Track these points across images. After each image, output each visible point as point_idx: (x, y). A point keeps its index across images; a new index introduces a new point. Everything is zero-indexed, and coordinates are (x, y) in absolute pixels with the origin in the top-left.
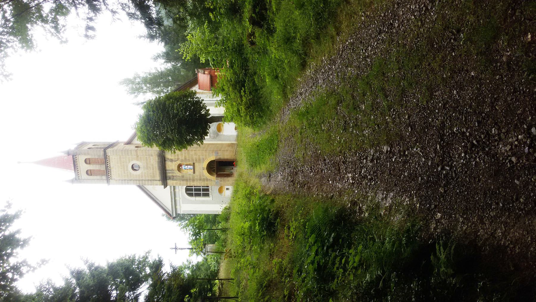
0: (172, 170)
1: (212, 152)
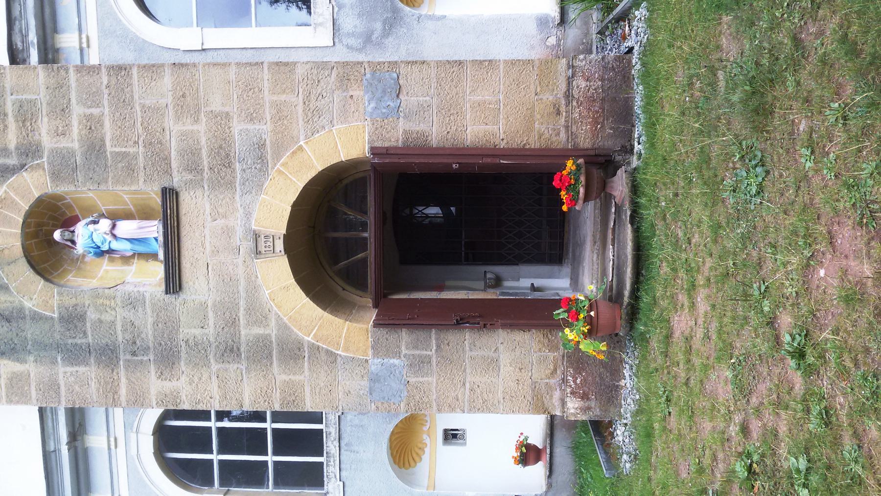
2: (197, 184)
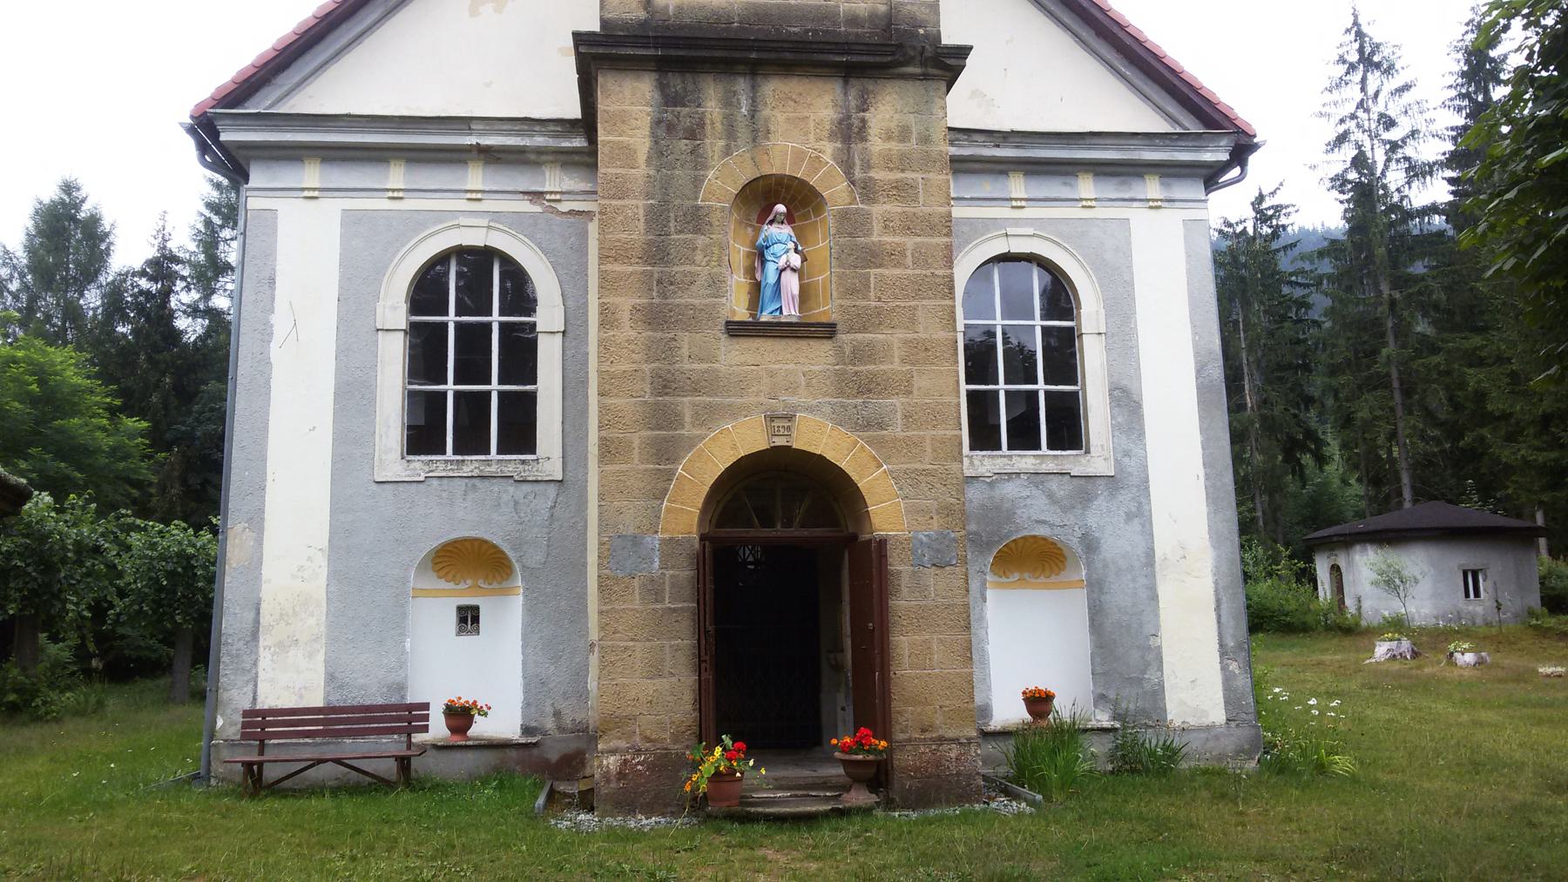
0: (759, 133)
1: (946, 511)
2: (840, 357)
